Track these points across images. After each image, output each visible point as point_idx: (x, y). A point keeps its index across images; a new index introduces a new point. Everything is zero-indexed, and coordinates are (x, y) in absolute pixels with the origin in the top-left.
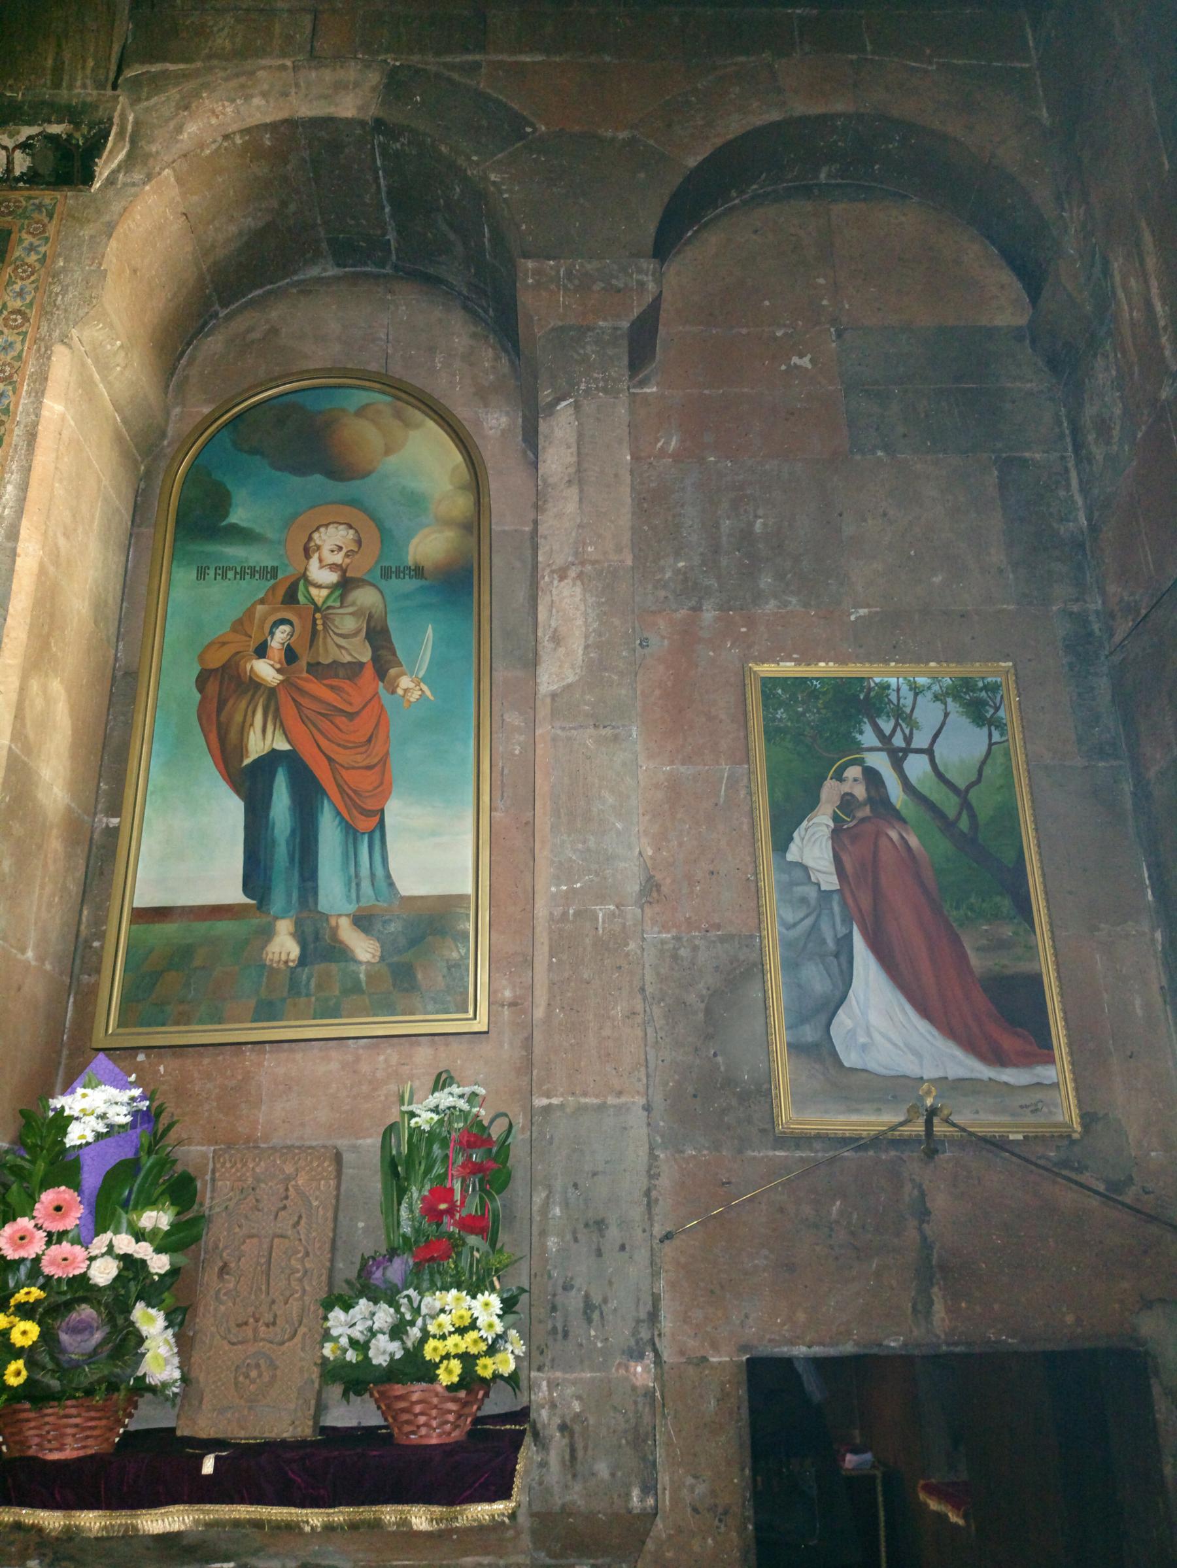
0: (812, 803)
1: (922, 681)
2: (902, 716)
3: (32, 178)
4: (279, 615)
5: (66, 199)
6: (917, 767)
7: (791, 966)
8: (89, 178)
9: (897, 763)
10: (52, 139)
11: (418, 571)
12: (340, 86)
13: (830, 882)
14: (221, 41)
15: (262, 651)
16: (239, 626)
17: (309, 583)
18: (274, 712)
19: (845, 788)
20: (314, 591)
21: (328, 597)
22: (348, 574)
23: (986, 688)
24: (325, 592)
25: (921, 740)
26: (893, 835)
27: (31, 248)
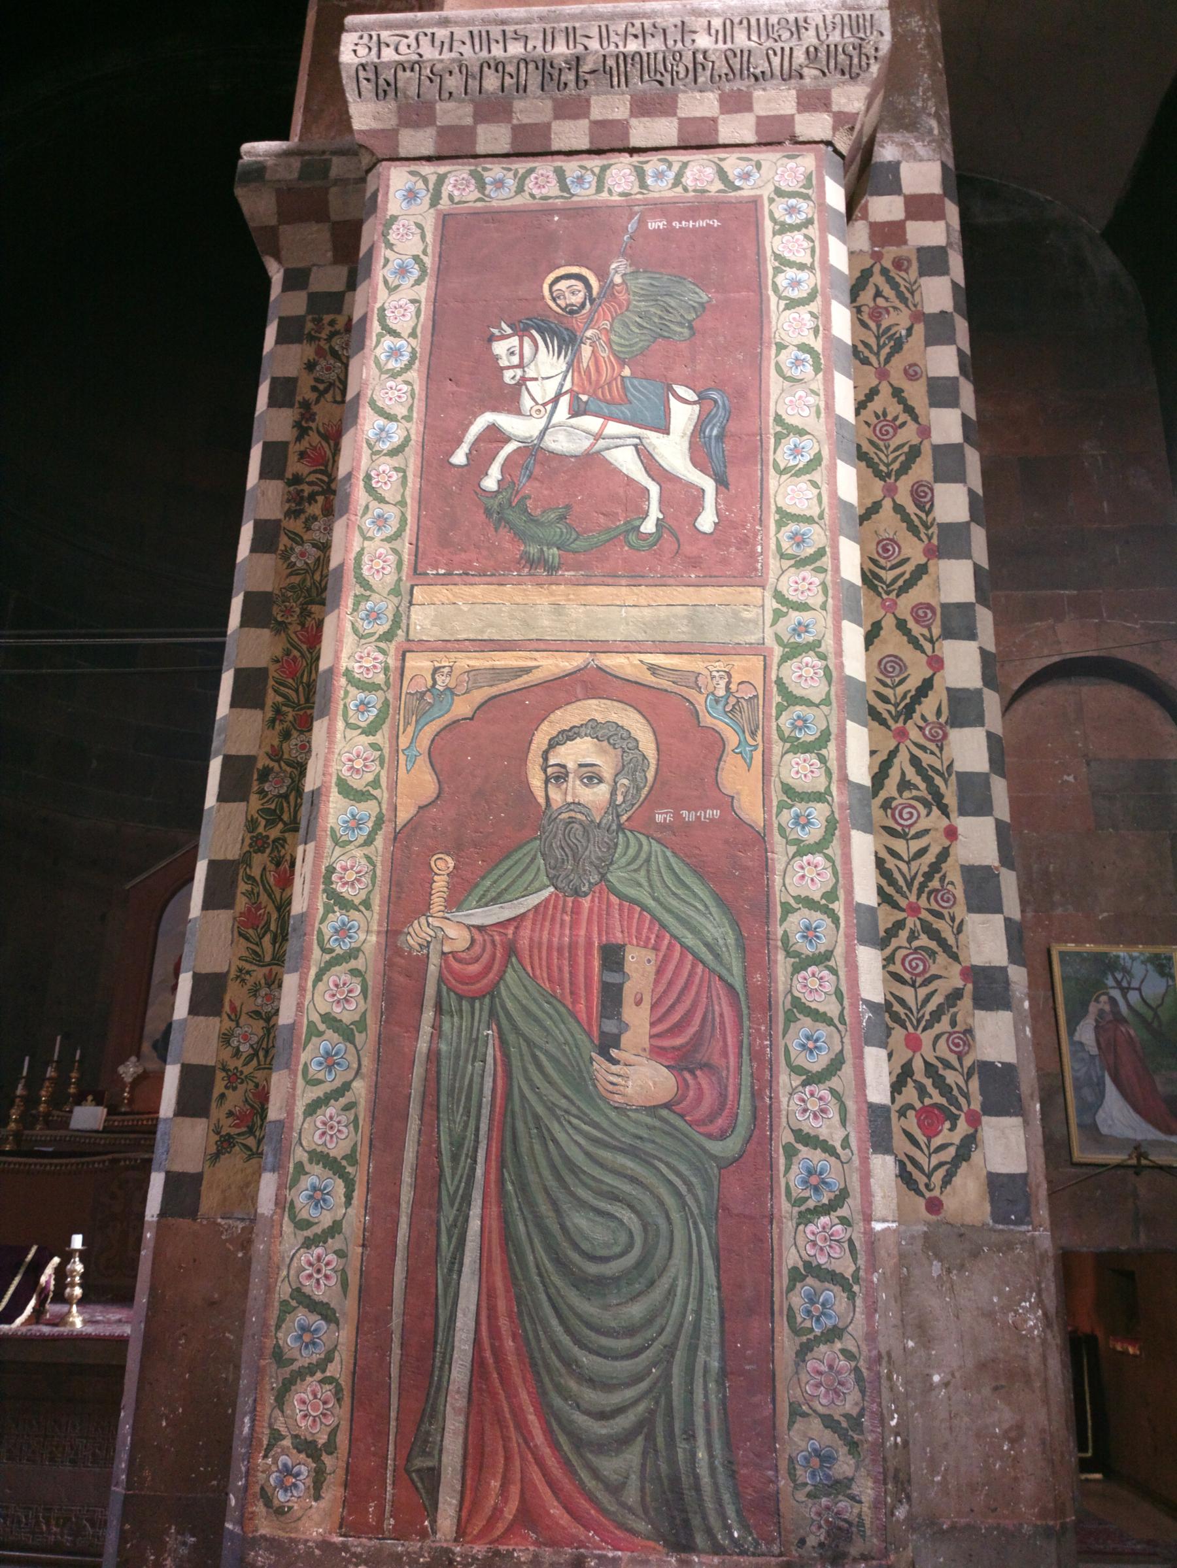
0: (1084, 1013)
1: (1135, 954)
2: (1126, 971)
6: (1133, 996)
7: (1077, 1089)
9: (1125, 996)
13: (1094, 1051)
19: (1100, 1006)
23: (1166, 958)
25: (1135, 984)
26: (1123, 1029)
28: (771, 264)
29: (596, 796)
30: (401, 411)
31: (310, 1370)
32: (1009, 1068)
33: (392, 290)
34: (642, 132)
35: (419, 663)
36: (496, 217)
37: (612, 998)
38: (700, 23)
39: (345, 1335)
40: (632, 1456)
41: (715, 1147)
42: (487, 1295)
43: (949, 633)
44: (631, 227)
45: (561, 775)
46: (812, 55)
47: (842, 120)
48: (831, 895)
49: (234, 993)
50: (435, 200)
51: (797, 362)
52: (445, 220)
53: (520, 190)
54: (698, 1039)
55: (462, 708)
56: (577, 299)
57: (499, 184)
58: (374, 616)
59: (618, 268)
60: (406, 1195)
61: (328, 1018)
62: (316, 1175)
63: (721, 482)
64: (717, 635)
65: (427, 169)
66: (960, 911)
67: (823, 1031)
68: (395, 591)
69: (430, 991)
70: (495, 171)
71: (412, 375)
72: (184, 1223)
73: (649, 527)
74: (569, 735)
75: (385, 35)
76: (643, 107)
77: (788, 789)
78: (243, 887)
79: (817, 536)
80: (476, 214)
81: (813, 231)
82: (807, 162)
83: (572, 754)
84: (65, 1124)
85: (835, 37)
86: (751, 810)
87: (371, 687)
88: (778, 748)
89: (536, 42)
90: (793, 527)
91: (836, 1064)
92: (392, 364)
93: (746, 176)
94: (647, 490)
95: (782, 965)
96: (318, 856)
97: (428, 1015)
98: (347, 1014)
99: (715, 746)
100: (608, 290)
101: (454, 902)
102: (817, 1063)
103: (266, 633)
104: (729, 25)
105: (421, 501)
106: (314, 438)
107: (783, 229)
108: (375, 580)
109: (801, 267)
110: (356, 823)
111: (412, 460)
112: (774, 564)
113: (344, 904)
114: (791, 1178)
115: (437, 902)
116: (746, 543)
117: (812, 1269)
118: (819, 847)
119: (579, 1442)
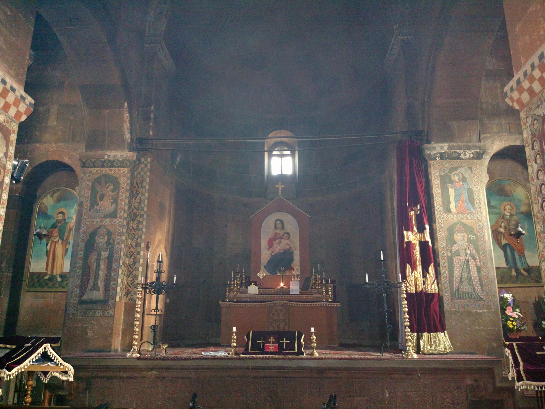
3: (473, 158)
4: (501, 221)
5: (478, 161)
8: (482, 158)
10: (477, 152)
11: (523, 213)
12: (516, 139)
14: (495, 130)
15: (501, 227)
16: (497, 222)
17: (506, 215)
18: (504, 237)
20: (507, 217)
21: (509, 218)
22: (512, 214)
24: (508, 217)
27: (476, 170)
84: (246, 292)
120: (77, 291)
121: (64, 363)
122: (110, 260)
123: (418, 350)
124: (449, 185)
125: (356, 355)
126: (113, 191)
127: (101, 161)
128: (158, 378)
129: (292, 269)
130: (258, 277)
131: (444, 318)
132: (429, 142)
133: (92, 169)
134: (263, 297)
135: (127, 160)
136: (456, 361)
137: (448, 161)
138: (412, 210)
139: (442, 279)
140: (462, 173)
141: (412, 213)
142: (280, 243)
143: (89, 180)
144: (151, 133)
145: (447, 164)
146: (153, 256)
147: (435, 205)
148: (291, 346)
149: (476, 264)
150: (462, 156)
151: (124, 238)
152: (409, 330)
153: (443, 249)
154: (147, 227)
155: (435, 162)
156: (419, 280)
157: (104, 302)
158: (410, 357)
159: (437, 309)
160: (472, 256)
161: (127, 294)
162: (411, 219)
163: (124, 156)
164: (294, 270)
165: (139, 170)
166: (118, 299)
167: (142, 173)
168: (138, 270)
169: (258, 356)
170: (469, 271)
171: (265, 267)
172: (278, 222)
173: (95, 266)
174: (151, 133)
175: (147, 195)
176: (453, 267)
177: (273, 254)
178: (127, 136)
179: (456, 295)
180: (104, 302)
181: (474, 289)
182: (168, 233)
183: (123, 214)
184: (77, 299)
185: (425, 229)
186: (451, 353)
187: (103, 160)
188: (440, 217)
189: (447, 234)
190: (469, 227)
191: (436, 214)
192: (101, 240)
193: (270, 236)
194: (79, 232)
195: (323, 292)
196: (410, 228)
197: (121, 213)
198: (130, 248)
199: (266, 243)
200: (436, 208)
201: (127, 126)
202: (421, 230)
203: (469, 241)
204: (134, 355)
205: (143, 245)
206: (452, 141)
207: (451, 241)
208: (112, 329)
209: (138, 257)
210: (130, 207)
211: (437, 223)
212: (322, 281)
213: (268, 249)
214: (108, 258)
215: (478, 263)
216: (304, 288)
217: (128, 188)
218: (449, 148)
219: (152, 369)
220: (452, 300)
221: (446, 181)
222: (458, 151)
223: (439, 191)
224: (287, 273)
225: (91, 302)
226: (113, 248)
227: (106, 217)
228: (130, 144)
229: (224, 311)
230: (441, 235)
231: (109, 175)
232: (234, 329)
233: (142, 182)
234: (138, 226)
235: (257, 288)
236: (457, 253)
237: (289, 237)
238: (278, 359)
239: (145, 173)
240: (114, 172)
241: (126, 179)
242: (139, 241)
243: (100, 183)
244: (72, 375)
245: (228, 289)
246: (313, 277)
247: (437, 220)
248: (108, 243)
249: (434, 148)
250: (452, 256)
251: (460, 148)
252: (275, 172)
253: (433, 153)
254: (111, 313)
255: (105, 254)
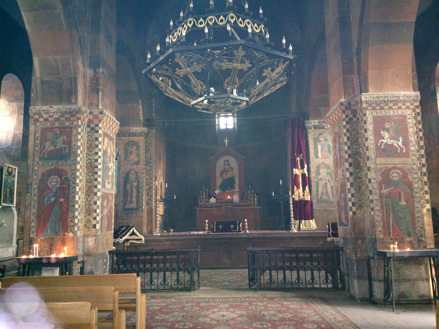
28: (408, 123)
29: (397, 179)
30: (372, 140)
31: (379, 226)
32: (428, 200)
33: (369, 126)
34: (394, 107)
35: (378, 166)
36: (379, 117)
37: (400, 196)
38: (400, 95)
39: (382, 223)
40: (405, 231)
41: (410, 208)
42: (393, 219)
43: (422, 158)
44: (393, 118)
45: (393, 177)
46: (412, 100)
47: (414, 106)
48: (418, 187)
49: (355, 195)
50: (372, 115)
51: (412, 134)
52: (374, 117)
53: (381, 114)
54: (408, 200)
55: (383, 170)
56: (389, 127)
57: (379, 113)
58: (373, 161)
59: (392, 123)
60: (385, 213)
61: (376, 199)
62: (377, 211)
63: (405, 147)
64: (406, 163)
65: (371, 111)
66: (424, 186)
67: (418, 199)
68: (375, 159)
69: (384, 196)
70: (378, 111)
71: (373, 135)
72: (355, 216)
73: (399, 152)
74: (393, 173)
75: (367, 96)
76: (394, 105)
77: (414, 178)
78: (354, 185)
79: (415, 153)
80: (376, 117)
81: (412, 119)
82: (411, 111)
83: (395, 175)
84: (209, 202)
85: (415, 98)
86: (411, 180)
87: (374, 169)
88: (413, 174)
89: (383, 98)
90: (412, 152)
91: (419, 201)
92: (371, 134)
93: (405, 112)
94: (398, 148)
95: (414, 193)
96: (372, 185)
97: (384, 199)
98: (377, 198)
99: (407, 174)
100: (392, 126)
101: (385, 189)
102: (418, 201)
103: (351, 159)
104: (404, 96)
105: (376, 149)
106: (352, 136)
107: (409, 119)
108: (372, 158)
109: (411, 123)
110: (375, 182)
111: (374, 145)
112: (411, 156)
113: (375, 189)
114: (416, 210)
115: (384, 189)
116: (408, 153)
117: (418, 217)
118: (417, 183)
119: (401, 230)
120: (122, 204)
121: (140, 235)
122: (138, 187)
123: (299, 229)
124: (318, 143)
125: (267, 232)
126: (136, 150)
127: (128, 133)
128: (171, 245)
129: (235, 188)
130: (216, 193)
131: (313, 213)
132: (308, 120)
133: (123, 138)
134: (219, 204)
135: (143, 133)
136: (316, 233)
137: (318, 129)
138: (298, 157)
139: (313, 193)
140: (325, 136)
141: (298, 159)
142: (227, 173)
143: (122, 144)
144: (154, 115)
145: (317, 131)
146: (158, 183)
147: (310, 154)
148: (235, 228)
149: (331, 185)
150: (325, 127)
151: (144, 175)
152: (293, 219)
153: (314, 177)
154: (155, 169)
155: (311, 130)
156: (301, 193)
157: (137, 209)
158: (293, 232)
159: (310, 209)
160: (329, 181)
161: (148, 204)
162: (298, 162)
163: (141, 130)
164: (235, 189)
165: (149, 137)
166: (144, 208)
167: (151, 139)
168: (152, 192)
169: (219, 233)
170: (327, 188)
171: (219, 187)
172: (226, 161)
173: (130, 190)
174: (154, 115)
175: (154, 151)
176: (319, 187)
177: (224, 180)
178: (142, 118)
179: (320, 201)
180: (137, 209)
181: (329, 198)
182: (163, 170)
183: (142, 162)
184: (122, 208)
185: (305, 167)
186: (316, 230)
187: (129, 133)
188: (312, 160)
189: (316, 169)
190: (328, 165)
191: (311, 159)
192: (132, 177)
193: (221, 170)
194: (120, 172)
195: (252, 201)
196: (297, 167)
197: (142, 162)
198: (147, 180)
199: (219, 174)
200: (311, 156)
201: (141, 112)
202: (302, 168)
203: (328, 173)
204: (158, 235)
205: (154, 178)
206: (320, 118)
207: (318, 173)
208: (142, 223)
209: (152, 185)
210: (146, 158)
211: (311, 164)
212: (251, 195)
213: (221, 177)
214: (137, 186)
215: (332, 184)
216: (241, 198)
217: (144, 148)
218: (319, 122)
219: (168, 241)
220: (317, 204)
221: (316, 140)
222: (323, 124)
223: (313, 146)
224: (232, 190)
225: (130, 209)
226: (139, 181)
227: (133, 164)
228: (143, 123)
229: (198, 213)
230: (313, 170)
231: (134, 141)
232: (207, 221)
233: (151, 144)
234: (150, 169)
235: (215, 199)
236: (321, 179)
237: (232, 170)
238: (229, 234)
239: (152, 138)
240: (136, 139)
241: (143, 143)
242: (152, 176)
243: (129, 146)
244: (144, 240)
245: (199, 201)
246: (247, 192)
247: (311, 162)
248: (136, 178)
249: (311, 123)
250: (318, 181)
251: (325, 123)
252: (222, 127)
253: (310, 125)
254: (141, 214)
255: (135, 184)
